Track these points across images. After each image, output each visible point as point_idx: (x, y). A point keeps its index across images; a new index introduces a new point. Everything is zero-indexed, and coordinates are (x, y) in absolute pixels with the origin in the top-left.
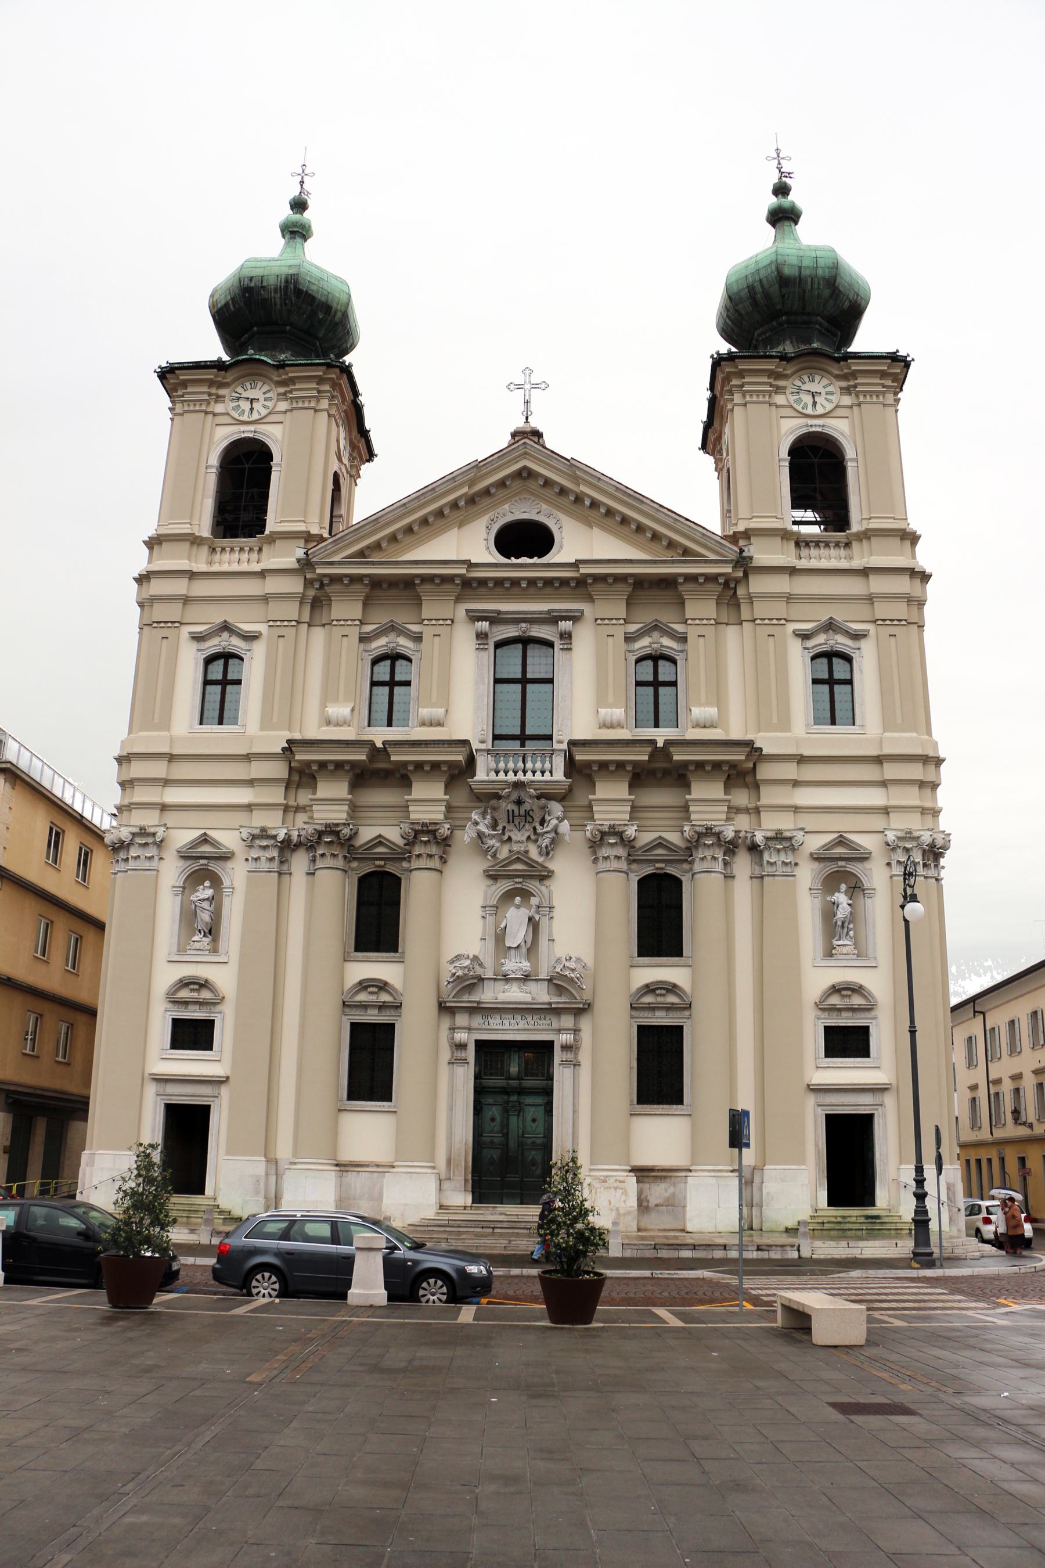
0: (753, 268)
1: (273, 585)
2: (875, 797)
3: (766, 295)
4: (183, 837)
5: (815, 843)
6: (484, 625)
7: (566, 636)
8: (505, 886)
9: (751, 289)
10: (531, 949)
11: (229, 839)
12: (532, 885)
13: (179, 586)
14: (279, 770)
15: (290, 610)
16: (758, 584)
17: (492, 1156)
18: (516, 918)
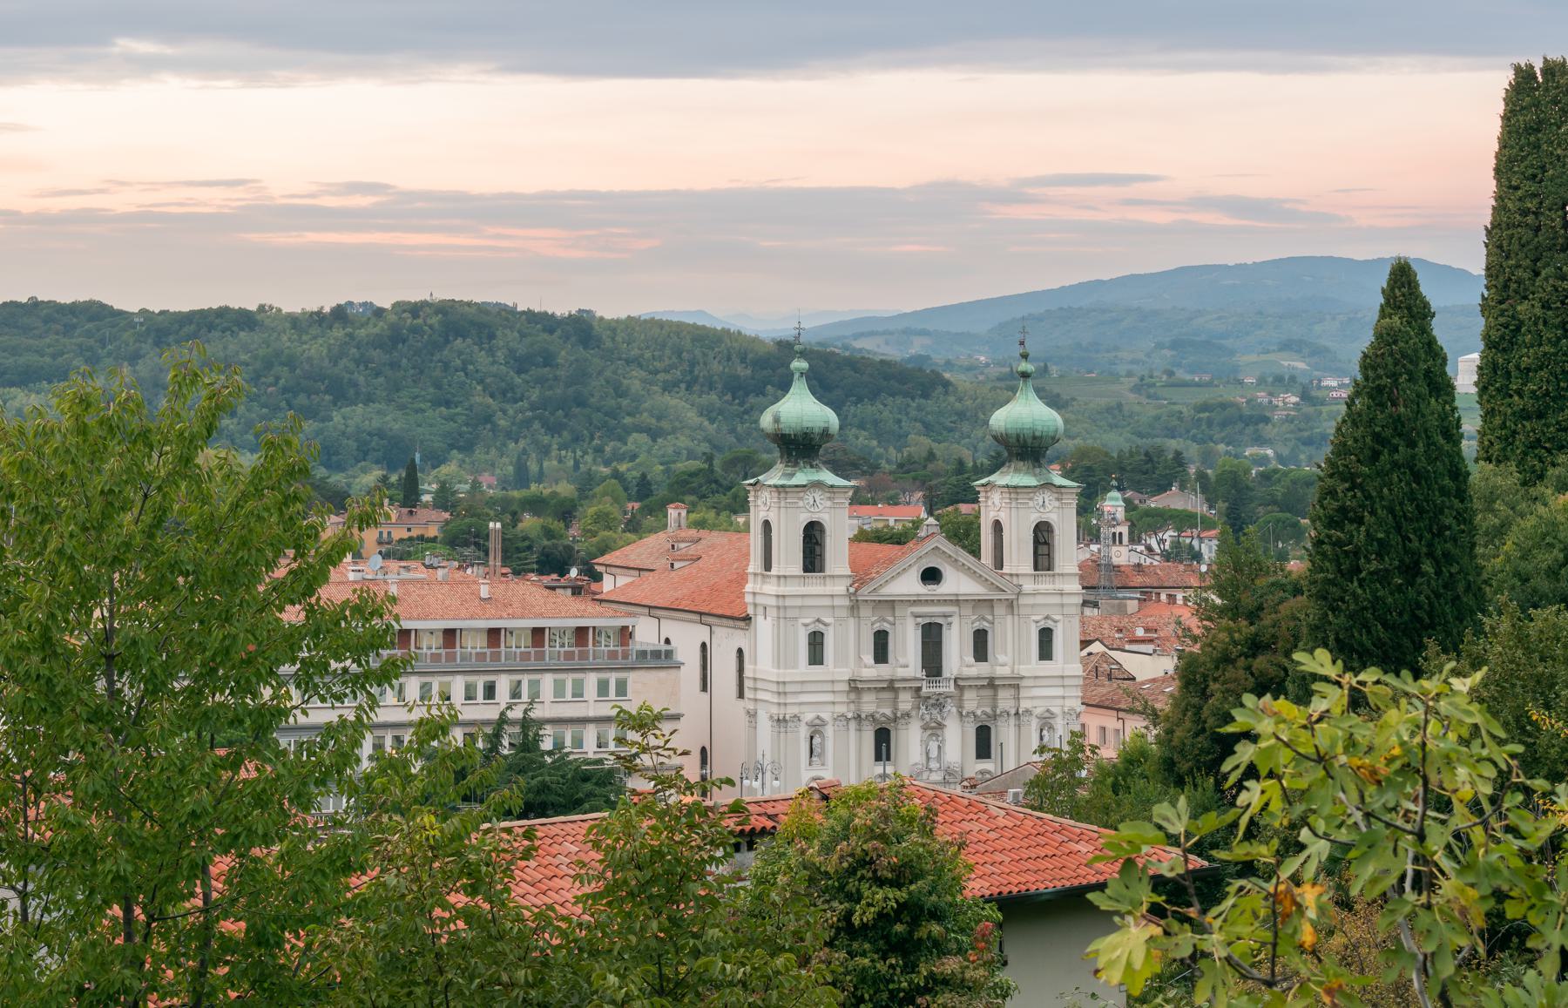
0: (1020, 426)
1: (837, 602)
2: (1059, 692)
3: (1025, 441)
4: (809, 716)
5: (1038, 711)
6: (919, 620)
7: (950, 624)
8: (929, 732)
9: (1018, 436)
10: (939, 758)
11: (826, 716)
12: (939, 732)
13: (798, 602)
14: (845, 687)
15: (844, 613)
16: (1023, 600)
17: (832, 829)
18: (933, 746)
